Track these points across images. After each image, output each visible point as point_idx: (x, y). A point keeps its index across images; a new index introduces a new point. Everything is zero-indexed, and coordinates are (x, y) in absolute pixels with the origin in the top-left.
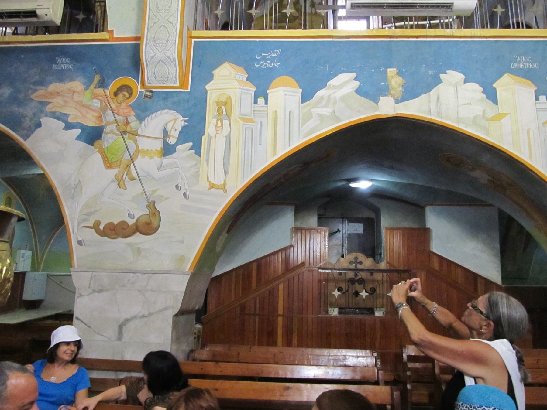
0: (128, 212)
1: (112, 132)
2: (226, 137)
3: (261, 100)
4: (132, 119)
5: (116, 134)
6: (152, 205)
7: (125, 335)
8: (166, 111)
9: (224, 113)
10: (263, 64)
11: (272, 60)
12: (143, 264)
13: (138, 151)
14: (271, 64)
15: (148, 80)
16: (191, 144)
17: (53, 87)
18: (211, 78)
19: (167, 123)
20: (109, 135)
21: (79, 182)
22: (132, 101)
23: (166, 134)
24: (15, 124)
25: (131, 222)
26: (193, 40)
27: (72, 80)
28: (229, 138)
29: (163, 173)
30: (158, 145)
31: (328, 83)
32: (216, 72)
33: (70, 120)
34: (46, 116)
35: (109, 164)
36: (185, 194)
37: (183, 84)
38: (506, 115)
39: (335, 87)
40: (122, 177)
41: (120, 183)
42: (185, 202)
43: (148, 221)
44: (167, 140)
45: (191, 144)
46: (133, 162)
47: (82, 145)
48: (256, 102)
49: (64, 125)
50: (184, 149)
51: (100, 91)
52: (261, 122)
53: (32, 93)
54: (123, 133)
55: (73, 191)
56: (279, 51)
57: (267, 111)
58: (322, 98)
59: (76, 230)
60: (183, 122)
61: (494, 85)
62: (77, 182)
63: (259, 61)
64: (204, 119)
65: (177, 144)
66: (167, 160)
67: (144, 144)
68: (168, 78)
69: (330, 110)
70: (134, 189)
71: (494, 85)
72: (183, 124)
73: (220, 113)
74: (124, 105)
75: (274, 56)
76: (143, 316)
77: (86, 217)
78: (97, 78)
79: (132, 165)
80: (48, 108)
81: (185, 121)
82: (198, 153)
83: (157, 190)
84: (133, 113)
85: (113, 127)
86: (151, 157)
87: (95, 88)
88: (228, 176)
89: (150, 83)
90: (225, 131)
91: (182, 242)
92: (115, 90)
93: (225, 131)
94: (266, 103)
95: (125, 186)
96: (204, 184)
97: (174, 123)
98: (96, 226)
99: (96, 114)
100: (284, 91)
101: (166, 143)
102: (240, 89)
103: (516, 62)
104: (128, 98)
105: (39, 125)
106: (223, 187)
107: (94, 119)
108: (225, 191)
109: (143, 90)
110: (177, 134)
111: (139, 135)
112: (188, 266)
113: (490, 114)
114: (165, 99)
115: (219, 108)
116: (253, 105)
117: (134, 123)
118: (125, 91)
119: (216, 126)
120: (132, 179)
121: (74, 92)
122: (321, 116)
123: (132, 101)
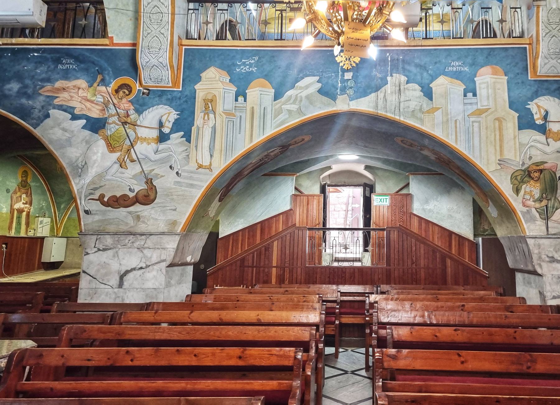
0: (129, 187)
1: (114, 122)
2: (212, 128)
3: (241, 99)
4: (131, 112)
5: (118, 125)
6: (149, 182)
7: (125, 283)
8: (161, 106)
9: (211, 108)
10: (243, 69)
11: (251, 65)
12: (142, 227)
13: (137, 138)
14: (249, 68)
15: (145, 80)
16: (182, 133)
17: (59, 84)
18: (199, 79)
19: (162, 116)
20: (112, 126)
21: (86, 163)
22: (132, 97)
23: (161, 125)
24: (25, 113)
25: (131, 195)
26: (184, 47)
27: (77, 78)
28: (214, 128)
29: (158, 156)
30: (155, 134)
31: (296, 85)
32: (203, 75)
33: (77, 112)
34: (54, 108)
35: (111, 148)
36: (177, 173)
37: (175, 84)
38: (438, 109)
39: (301, 88)
40: (124, 160)
41: (122, 164)
42: (178, 179)
43: (146, 194)
44: (162, 129)
45: (182, 133)
46: (133, 147)
47: (87, 133)
48: (236, 100)
49: (70, 116)
50: (176, 137)
51: (103, 88)
52: (241, 116)
53: (41, 88)
54: (124, 123)
55: (80, 170)
56: (256, 58)
57: (246, 107)
58: (290, 97)
59: (83, 202)
60: (176, 116)
61: (431, 85)
62: (83, 164)
63: (240, 66)
64: (193, 113)
65: (170, 133)
66: (162, 146)
67: (142, 132)
68: (162, 79)
69: (297, 107)
70: (133, 169)
71: (431, 85)
72: (176, 117)
73: (206, 108)
74: (124, 100)
75: (252, 62)
76: (141, 268)
77: (92, 191)
78: (99, 78)
79: (132, 149)
80: (56, 102)
81: (177, 115)
82: (189, 141)
83: (154, 170)
84: (132, 107)
85: (115, 119)
86: (149, 144)
87: (98, 85)
88: (213, 159)
89: (146, 83)
90: (211, 123)
91: (175, 210)
92: (116, 88)
93: (211, 123)
94: (245, 101)
95: (126, 167)
96: (193, 166)
97: (168, 116)
98: (101, 199)
99: (100, 108)
100: (260, 91)
101: (161, 132)
102: (224, 89)
103: (450, 66)
104: (127, 95)
105: (47, 116)
106: (209, 168)
107: (98, 112)
108: (211, 170)
109: (141, 88)
110: (170, 125)
111: (138, 126)
112: (179, 229)
113: (425, 108)
114: (160, 96)
115: (206, 104)
116: (234, 102)
117: (133, 116)
118: (125, 89)
119: (204, 119)
120: (133, 161)
121: (79, 88)
122: (290, 112)
123: (132, 97)
